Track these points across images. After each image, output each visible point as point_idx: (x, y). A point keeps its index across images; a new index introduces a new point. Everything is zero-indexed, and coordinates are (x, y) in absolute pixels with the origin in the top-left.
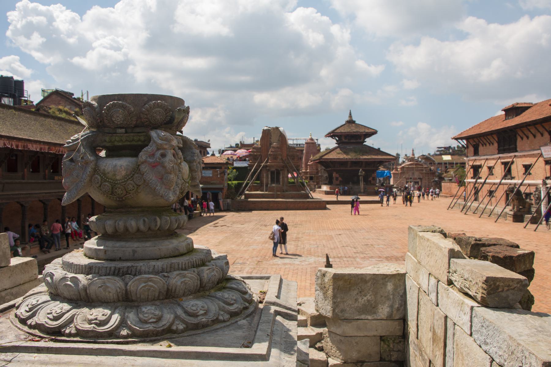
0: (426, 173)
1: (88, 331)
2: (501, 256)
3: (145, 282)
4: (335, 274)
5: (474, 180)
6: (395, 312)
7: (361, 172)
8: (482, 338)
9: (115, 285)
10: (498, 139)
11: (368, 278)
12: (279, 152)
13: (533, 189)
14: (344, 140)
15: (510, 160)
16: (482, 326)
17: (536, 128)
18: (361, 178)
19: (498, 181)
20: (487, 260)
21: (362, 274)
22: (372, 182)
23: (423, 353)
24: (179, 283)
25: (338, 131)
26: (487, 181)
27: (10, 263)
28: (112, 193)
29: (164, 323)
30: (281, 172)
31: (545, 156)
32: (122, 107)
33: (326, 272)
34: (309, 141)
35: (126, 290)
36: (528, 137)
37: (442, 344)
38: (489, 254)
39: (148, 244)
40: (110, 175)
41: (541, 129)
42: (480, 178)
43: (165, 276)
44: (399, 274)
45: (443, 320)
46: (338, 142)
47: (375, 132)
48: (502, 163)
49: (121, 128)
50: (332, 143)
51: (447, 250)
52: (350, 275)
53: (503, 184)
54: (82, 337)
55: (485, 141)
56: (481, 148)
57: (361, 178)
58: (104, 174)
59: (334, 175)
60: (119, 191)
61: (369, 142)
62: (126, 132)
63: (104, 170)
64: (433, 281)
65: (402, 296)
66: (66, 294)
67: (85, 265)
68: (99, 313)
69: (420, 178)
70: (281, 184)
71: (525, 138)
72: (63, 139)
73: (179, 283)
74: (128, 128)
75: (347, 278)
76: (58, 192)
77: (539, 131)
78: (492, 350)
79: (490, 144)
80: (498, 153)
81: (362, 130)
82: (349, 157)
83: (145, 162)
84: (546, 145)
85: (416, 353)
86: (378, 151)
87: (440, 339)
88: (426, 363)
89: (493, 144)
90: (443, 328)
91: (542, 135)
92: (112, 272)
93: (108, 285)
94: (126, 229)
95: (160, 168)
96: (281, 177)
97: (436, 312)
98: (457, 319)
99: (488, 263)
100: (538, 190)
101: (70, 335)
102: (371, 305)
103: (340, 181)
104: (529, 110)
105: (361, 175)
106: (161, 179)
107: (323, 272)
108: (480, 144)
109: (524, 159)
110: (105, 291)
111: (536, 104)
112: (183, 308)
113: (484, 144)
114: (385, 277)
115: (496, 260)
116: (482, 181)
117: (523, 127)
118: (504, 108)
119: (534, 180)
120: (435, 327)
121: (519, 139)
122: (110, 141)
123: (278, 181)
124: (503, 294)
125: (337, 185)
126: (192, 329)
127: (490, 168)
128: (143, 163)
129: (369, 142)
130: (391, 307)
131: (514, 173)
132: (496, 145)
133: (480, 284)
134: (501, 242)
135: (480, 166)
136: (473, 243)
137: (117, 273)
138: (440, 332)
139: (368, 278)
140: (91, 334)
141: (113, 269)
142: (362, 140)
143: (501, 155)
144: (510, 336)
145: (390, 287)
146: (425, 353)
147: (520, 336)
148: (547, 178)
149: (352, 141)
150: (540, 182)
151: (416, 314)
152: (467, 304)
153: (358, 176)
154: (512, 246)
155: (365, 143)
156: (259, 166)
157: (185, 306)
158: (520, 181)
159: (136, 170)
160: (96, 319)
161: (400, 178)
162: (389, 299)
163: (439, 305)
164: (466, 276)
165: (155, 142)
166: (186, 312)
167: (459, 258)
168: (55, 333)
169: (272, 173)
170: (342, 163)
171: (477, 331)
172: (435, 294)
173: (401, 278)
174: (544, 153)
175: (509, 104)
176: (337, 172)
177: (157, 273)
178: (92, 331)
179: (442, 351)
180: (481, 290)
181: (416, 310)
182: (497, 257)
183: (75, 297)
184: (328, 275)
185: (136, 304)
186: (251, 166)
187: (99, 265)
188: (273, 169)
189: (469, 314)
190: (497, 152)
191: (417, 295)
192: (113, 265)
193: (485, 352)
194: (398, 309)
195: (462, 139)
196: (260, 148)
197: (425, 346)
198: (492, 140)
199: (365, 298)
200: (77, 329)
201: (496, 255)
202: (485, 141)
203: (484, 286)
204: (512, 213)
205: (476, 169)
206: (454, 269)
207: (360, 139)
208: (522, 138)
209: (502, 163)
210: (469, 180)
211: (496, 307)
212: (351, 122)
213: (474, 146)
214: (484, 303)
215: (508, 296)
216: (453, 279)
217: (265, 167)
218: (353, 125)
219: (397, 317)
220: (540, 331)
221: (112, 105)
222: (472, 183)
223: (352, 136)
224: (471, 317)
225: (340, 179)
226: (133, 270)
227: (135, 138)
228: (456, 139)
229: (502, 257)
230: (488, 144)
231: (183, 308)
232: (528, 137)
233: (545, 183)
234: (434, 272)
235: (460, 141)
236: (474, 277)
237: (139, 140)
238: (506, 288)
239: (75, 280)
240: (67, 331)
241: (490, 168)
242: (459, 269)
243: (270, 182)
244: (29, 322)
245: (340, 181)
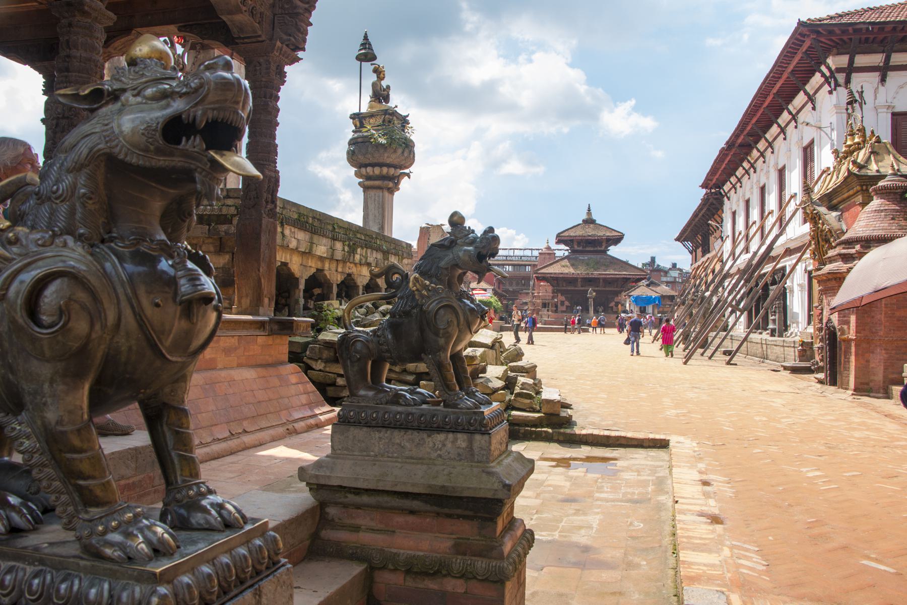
7: (591, 293)
18: (591, 302)
25: (566, 234)
34: (545, 251)
46: (574, 251)
57: (591, 302)
86: (625, 265)
103: (567, 307)
125: (563, 312)
142: (603, 248)
149: (587, 249)
153: (588, 299)
170: (570, 281)
176: (563, 293)
207: (601, 246)
212: (589, 221)
218: (591, 226)
223: (590, 242)
225: (567, 303)
245: (567, 307)
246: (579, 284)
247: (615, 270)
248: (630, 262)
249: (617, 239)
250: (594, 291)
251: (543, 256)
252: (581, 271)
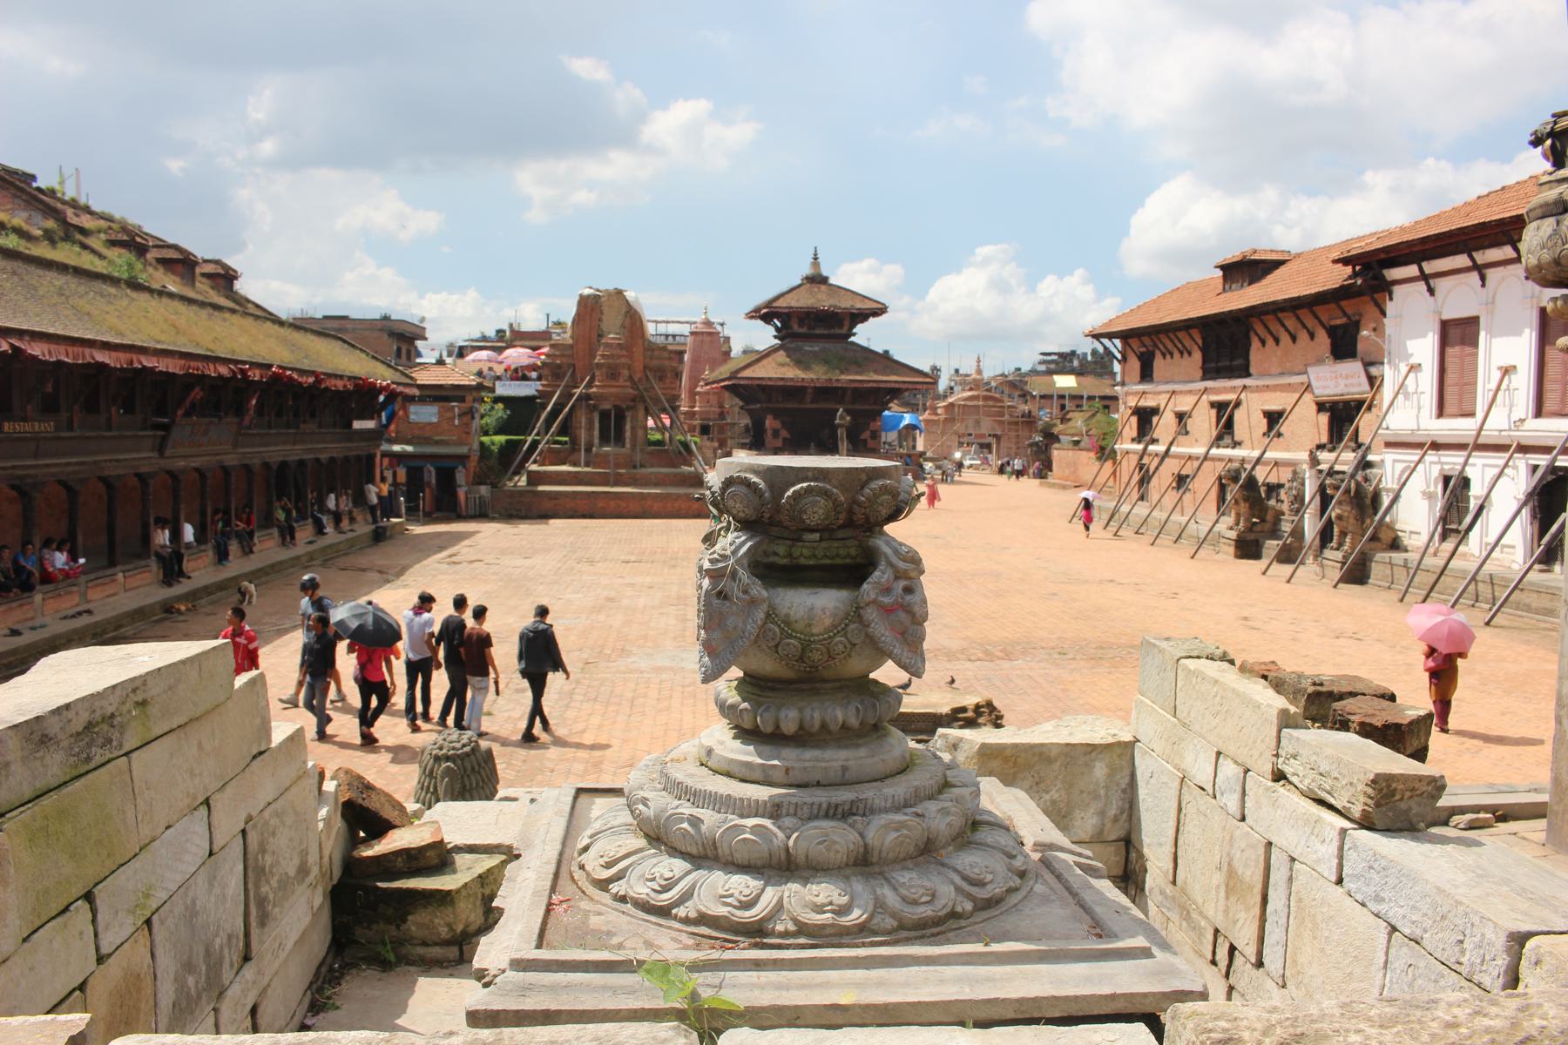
0: (1010, 423)
1: (823, 926)
2: (1378, 722)
3: (897, 830)
4: (984, 746)
5: (1140, 447)
6: (1109, 825)
7: (842, 418)
8: (1371, 890)
9: (841, 838)
10: (1204, 339)
11: (1054, 752)
12: (623, 360)
13: (1284, 476)
14: (796, 328)
15: (1232, 397)
16: (1371, 867)
17: (1298, 318)
19: (1200, 450)
20: (1348, 730)
21: (1042, 745)
22: (871, 443)
23: (1194, 915)
24: (943, 827)
26: (1173, 449)
27: (270, 741)
28: (801, 659)
29: (943, 902)
30: (629, 414)
31: (1317, 392)
32: (826, 494)
33: (961, 740)
34: (701, 328)
35: (866, 846)
36: (1277, 341)
37: (1258, 899)
38: (1352, 718)
39: (862, 752)
40: (800, 626)
41: (1310, 322)
42: (1154, 441)
43: (918, 815)
44: (1119, 743)
45: (1261, 851)
46: (782, 334)
47: (879, 311)
48: (1213, 405)
49: (812, 531)
50: (764, 336)
51: (1275, 713)
52: (1016, 745)
53: (1213, 459)
54: (809, 936)
55: (1170, 346)
56: (1159, 363)
58: (787, 622)
59: (769, 422)
60: (816, 656)
61: (866, 335)
62: (821, 540)
63: (788, 615)
64: (1229, 770)
65: (1124, 791)
66: (739, 857)
67: (765, 803)
68: (824, 891)
69: (995, 436)
70: (628, 445)
71: (1270, 342)
72: (26, 314)
73: (943, 827)
74: (826, 531)
75: (1008, 752)
76: (14, 467)
77: (1304, 326)
78: (1395, 914)
80: (1204, 378)
81: (845, 303)
82: (812, 376)
83: (874, 602)
84: (1320, 361)
85: (1169, 914)
87: (1251, 888)
88: (1201, 935)
89: (1190, 354)
90: (1261, 866)
91: (1312, 336)
92: (822, 813)
93: (836, 838)
94: (824, 726)
95: (902, 615)
96: (628, 427)
97: (1238, 833)
98: (1299, 850)
99: (1351, 737)
100: (1296, 476)
101: (786, 934)
102: (1059, 811)
104: (1282, 269)
105: (840, 426)
106: (902, 634)
107: (951, 740)
108: (1158, 355)
109: (1267, 395)
110: (828, 850)
111: (1298, 255)
112: (956, 870)
114: (1091, 749)
115: (1367, 731)
116: (1160, 448)
117: (1267, 313)
118: (1220, 260)
119: (1287, 450)
120: (1236, 863)
121: (1255, 344)
122: (790, 555)
123: (620, 439)
124: (1403, 805)
126: (983, 909)
127: (1181, 417)
128: (868, 604)
129: (866, 335)
130: (1102, 813)
131: (1240, 430)
132: (1197, 356)
133: (1361, 787)
134: (1359, 687)
135: (1155, 411)
136: (1311, 689)
137: (834, 813)
138: (1253, 875)
139: (1054, 752)
140: (828, 931)
141: (824, 806)
142: (844, 331)
143: (1209, 384)
144: (1438, 888)
145: (1100, 770)
146: (1201, 913)
147: (1457, 887)
148: (1320, 447)
149: (818, 331)
150: (1305, 456)
151: (1172, 832)
152: (1330, 824)
153: (834, 428)
154: (1383, 696)
155: (852, 339)
156: (567, 396)
157: (960, 868)
158: (1256, 454)
159: (856, 614)
160: (831, 903)
161: (943, 433)
162: (1096, 797)
163: (1248, 819)
164: (1324, 767)
165: (890, 564)
166: (965, 878)
167: (1296, 727)
168: (757, 932)
169: (604, 416)
171: (1357, 877)
172: (1237, 796)
173: (1125, 751)
174: (1314, 383)
175: (1232, 254)
176: (777, 414)
177: (897, 809)
178: (832, 925)
179: (1257, 911)
180: (1362, 799)
181: (1173, 823)
182: (1371, 725)
183: (759, 863)
184: (966, 747)
185: (877, 869)
186: (545, 396)
187: (794, 800)
188: (606, 406)
189: (1336, 844)
190: (1200, 373)
191: (1174, 793)
192: (821, 797)
193: (1377, 915)
194: (1116, 819)
195: (1110, 336)
196: (571, 346)
197: (1200, 901)
198: (1188, 343)
199: (1047, 797)
200: (795, 921)
201: (1368, 720)
202: (1170, 346)
203: (1370, 791)
204: (1233, 534)
205: (1145, 417)
206: (1291, 751)
207: (841, 327)
208: (1263, 342)
209: (1213, 405)
210: (1126, 444)
211: (1389, 830)
213: (1141, 357)
214: (1366, 823)
215: (1410, 809)
216: (1287, 770)
217: (585, 397)
218: (823, 287)
219: (1113, 837)
220: (1481, 876)
221: (808, 490)
222: (1135, 452)
223: (817, 321)
224: (1341, 848)
225: (784, 433)
226: (861, 806)
227: (841, 552)
228: (1097, 337)
229: (1379, 724)
230: (1177, 355)
231: (956, 870)
232: (1277, 341)
233: (1314, 461)
234: (1230, 749)
235: (1106, 341)
236: (1345, 771)
237: (848, 556)
238: (1408, 794)
239: (695, 821)
240: (780, 928)
241: (1181, 417)
242: (1304, 752)
243: (596, 441)
244: (681, 912)
246: (808, 398)
247: (876, 372)
248: (898, 356)
250: (847, 411)
251: (699, 338)
252: (815, 375)
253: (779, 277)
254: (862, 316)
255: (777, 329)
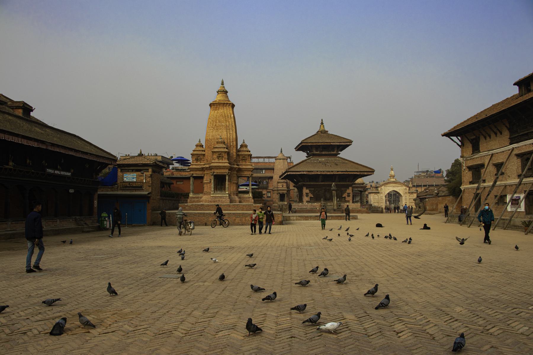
25: (309, 141)
48: (518, 155)
50: (302, 156)
61: (343, 154)
79: (496, 134)
80: (511, 144)
89: (501, 133)
103: (311, 198)
108: (482, 138)
113: (487, 136)
118: (517, 80)
132: (506, 134)
135: (482, 166)
142: (335, 153)
155: (338, 155)
190: (508, 141)
209: (518, 155)
212: (323, 132)
213: (472, 141)
225: (311, 195)
230: (493, 135)
241: (499, 166)
245: (311, 198)
249: (345, 145)
253: (308, 131)
254: (343, 147)
255: (308, 154)
